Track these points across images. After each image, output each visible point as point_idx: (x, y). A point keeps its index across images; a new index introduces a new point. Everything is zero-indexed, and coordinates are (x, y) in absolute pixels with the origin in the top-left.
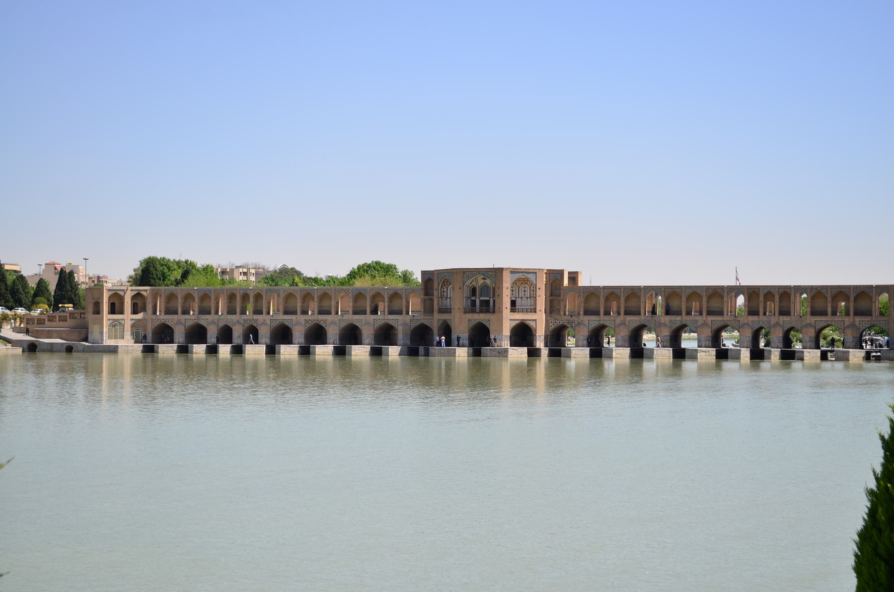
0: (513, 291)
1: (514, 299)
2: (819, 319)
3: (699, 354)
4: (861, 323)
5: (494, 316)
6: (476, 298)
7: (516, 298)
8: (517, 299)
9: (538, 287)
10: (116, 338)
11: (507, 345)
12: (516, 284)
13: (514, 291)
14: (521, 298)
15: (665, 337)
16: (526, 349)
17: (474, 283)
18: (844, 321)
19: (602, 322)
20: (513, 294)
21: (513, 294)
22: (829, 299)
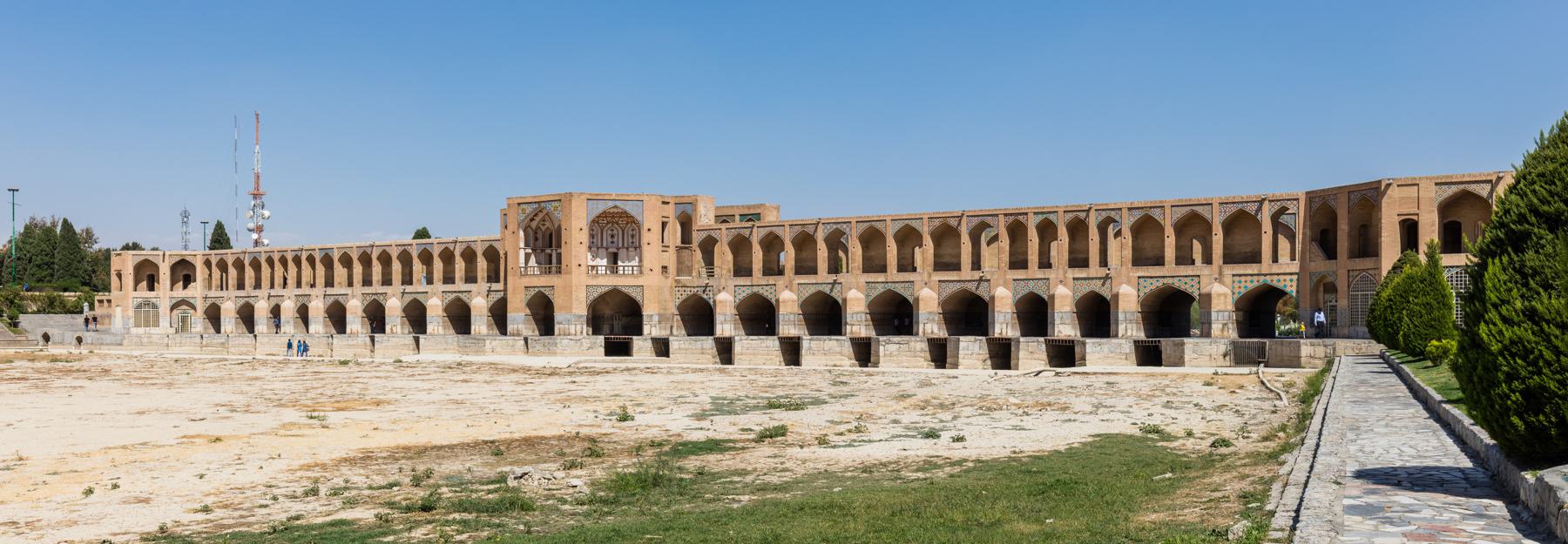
0: (593, 238)
1: (615, 250)
2: (1149, 275)
3: (881, 348)
4: (1237, 279)
5: (559, 280)
6: (552, 250)
7: (618, 249)
8: (621, 250)
9: (646, 228)
10: (147, 325)
11: (582, 333)
12: (598, 222)
13: (616, 237)
14: (627, 249)
15: (855, 316)
16: (603, 337)
17: (548, 224)
18: (1199, 276)
19: (755, 289)
20: (612, 242)
21: (593, 243)
22: (1170, 233)
